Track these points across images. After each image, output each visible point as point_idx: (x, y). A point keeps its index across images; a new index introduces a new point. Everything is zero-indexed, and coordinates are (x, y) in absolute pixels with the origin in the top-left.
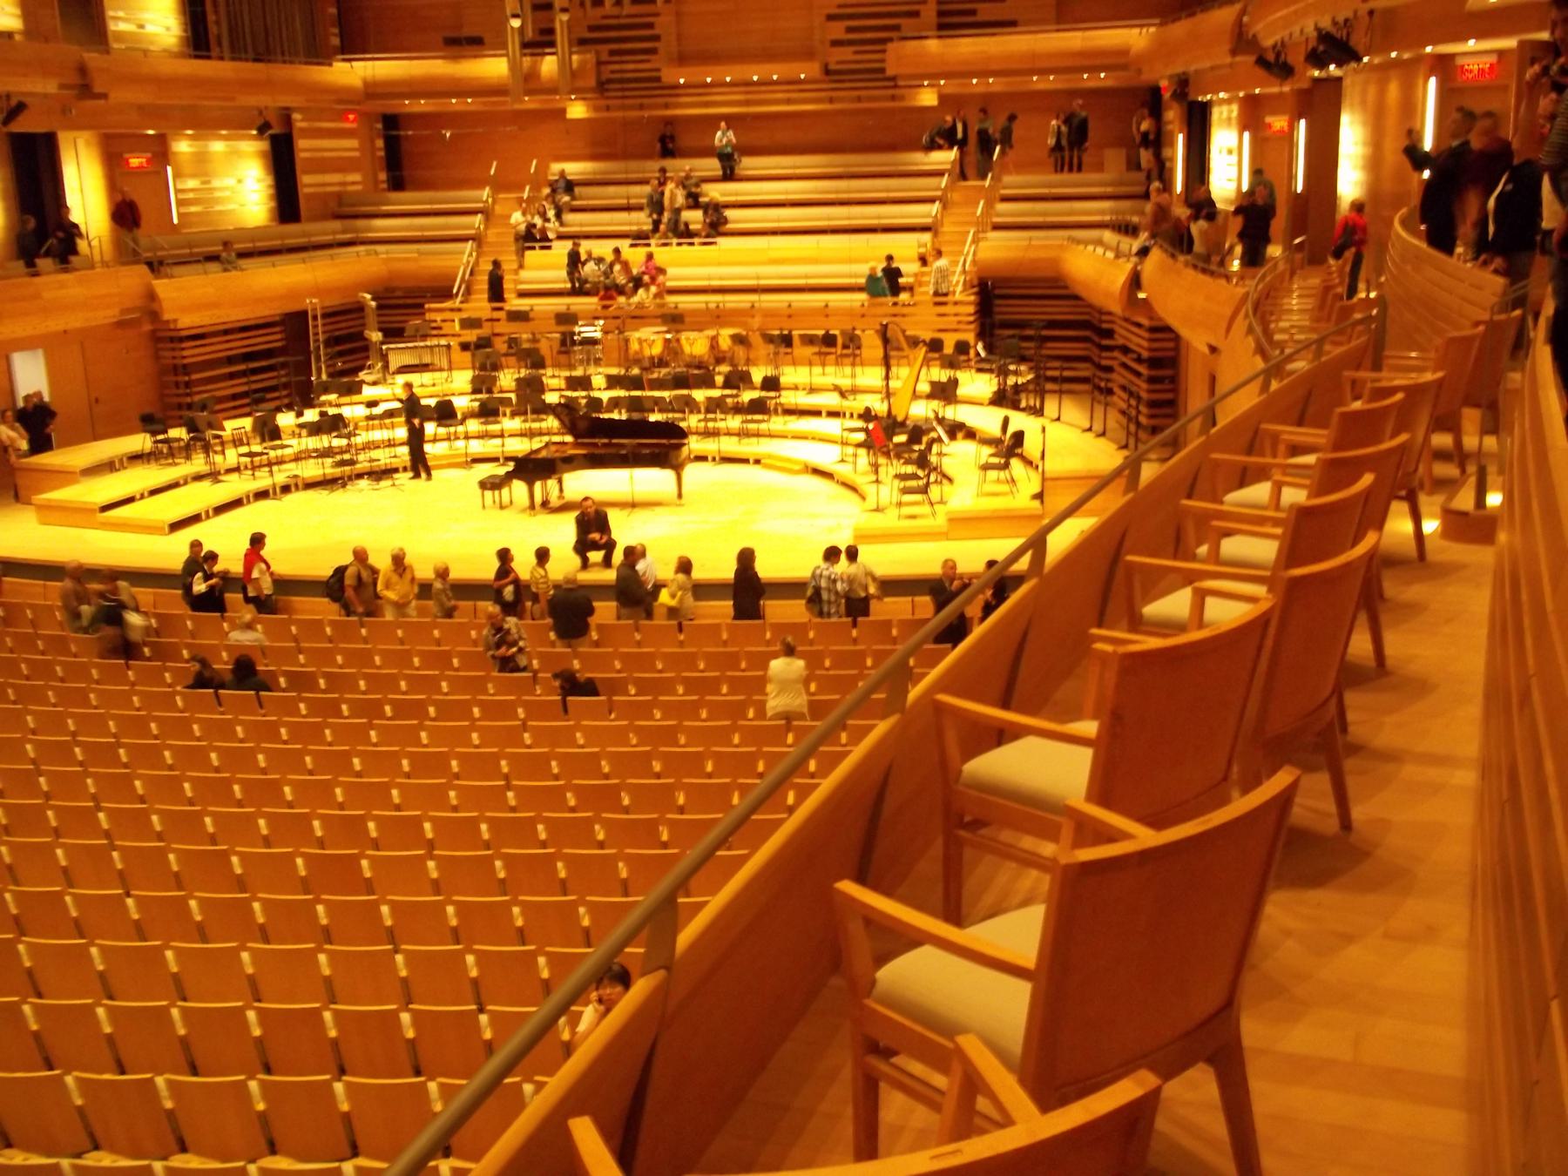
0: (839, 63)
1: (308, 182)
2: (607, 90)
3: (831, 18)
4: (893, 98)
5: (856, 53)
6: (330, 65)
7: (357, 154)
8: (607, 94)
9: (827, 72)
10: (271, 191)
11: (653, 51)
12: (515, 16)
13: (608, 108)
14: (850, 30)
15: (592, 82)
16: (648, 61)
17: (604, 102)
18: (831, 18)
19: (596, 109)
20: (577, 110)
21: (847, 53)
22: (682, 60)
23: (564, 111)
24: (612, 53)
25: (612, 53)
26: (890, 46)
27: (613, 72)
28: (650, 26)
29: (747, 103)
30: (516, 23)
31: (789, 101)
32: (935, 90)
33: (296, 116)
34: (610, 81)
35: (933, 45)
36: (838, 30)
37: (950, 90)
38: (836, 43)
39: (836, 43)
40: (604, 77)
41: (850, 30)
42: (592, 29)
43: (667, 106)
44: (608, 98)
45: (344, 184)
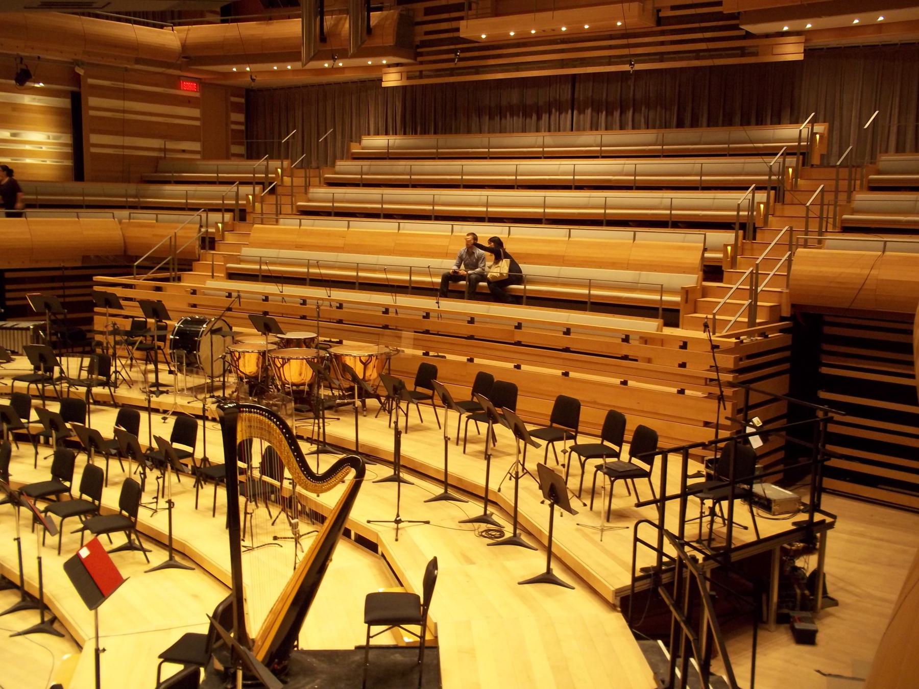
0: (674, 8)
1: (98, 143)
2: (421, 54)
4: (742, 52)
6: (162, 27)
7: (198, 123)
8: (419, 59)
9: (659, 21)
10: (69, 150)
13: (421, 76)
15: (390, 41)
19: (408, 78)
20: (392, 79)
23: (381, 80)
27: (427, 33)
29: (563, 64)
31: (610, 61)
32: (802, 39)
33: (81, 71)
34: (424, 44)
37: (820, 42)
40: (418, 39)
43: (477, 70)
44: (421, 63)
45: (165, 150)
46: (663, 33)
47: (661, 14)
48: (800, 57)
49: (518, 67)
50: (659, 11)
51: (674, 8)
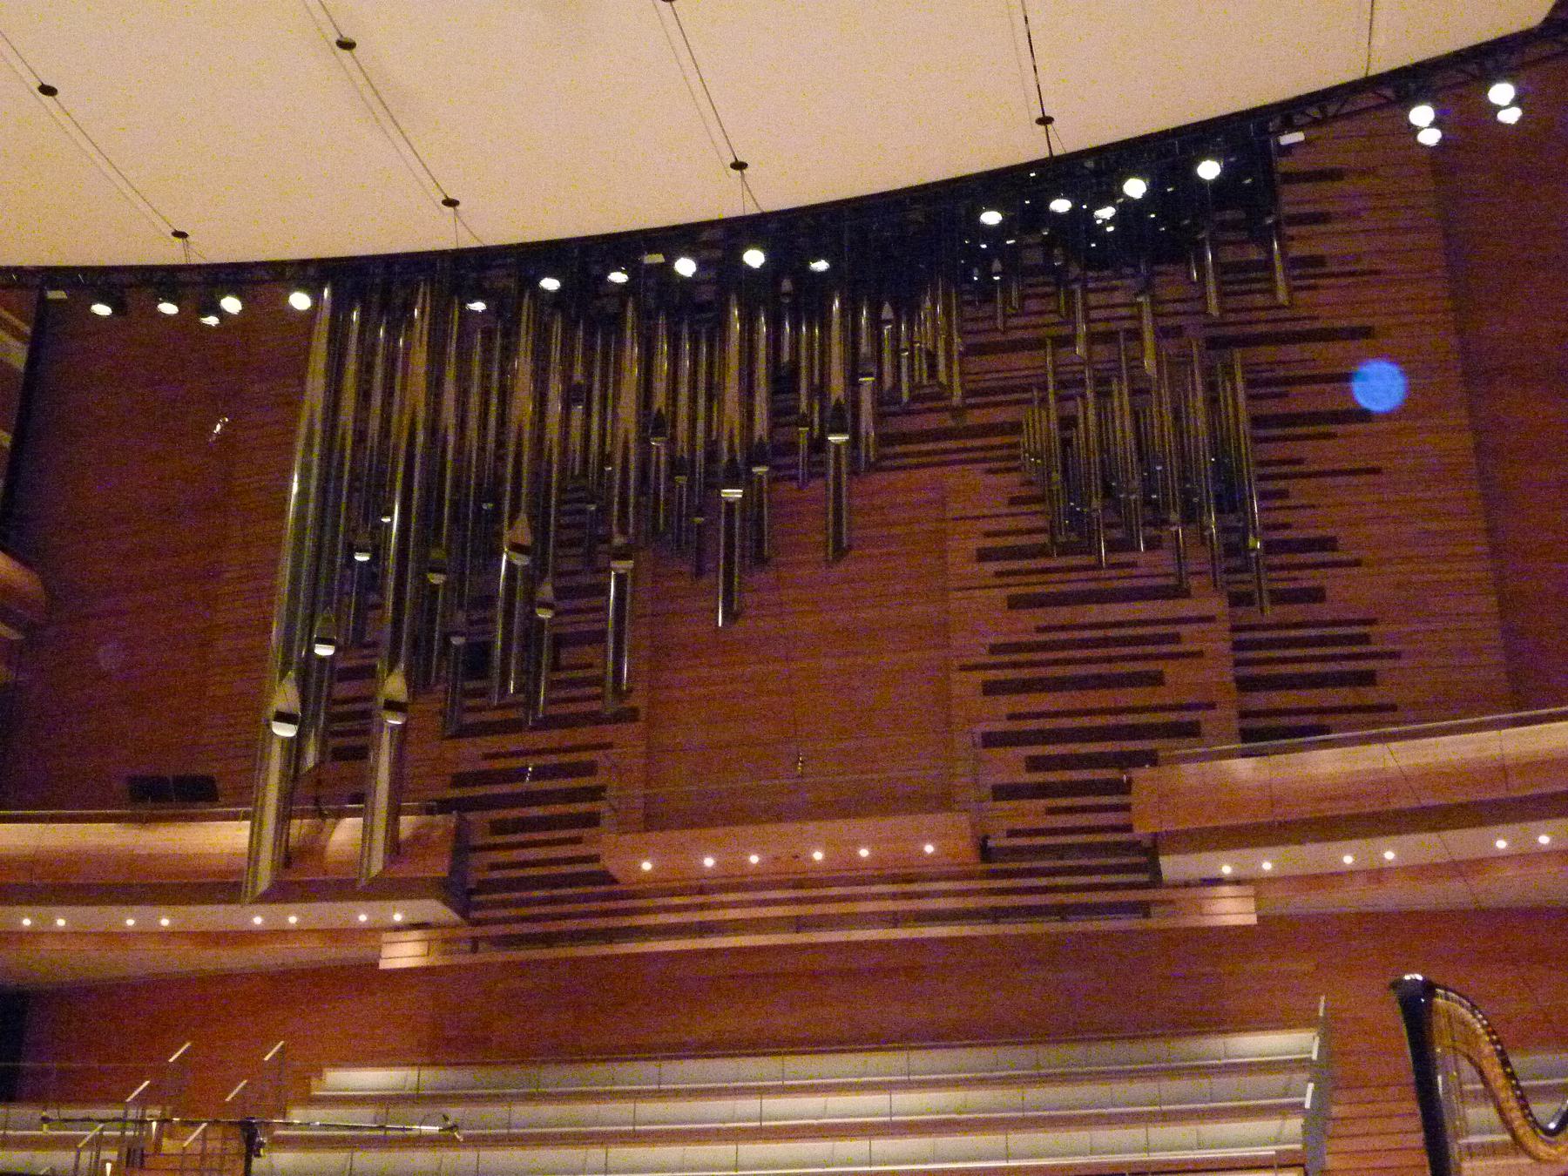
0: (1012, 833)
2: (480, 906)
3: (990, 740)
5: (1052, 811)
8: (476, 915)
9: (985, 853)
11: (592, 820)
12: (283, 717)
14: (1035, 764)
16: (577, 841)
17: (467, 932)
18: (990, 740)
20: (404, 954)
21: (1031, 812)
22: (653, 819)
24: (499, 828)
25: (499, 828)
26: (1142, 774)
27: (495, 867)
28: (589, 769)
29: (800, 924)
30: (285, 731)
31: (895, 920)
32: (1250, 890)
34: (486, 886)
35: (1243, 768)
36: (1009, 765)
38: (1006, 792)
39: (1006, 792)
40: (474, 877)
41: (1035, 764)
42: (460, 780)
43: (610, 936)
46: (994, 875)
47: (991, 843)
48: (1252, 920)
49: (705, 929)
50: (986, 838)
51: (1012, 833)
